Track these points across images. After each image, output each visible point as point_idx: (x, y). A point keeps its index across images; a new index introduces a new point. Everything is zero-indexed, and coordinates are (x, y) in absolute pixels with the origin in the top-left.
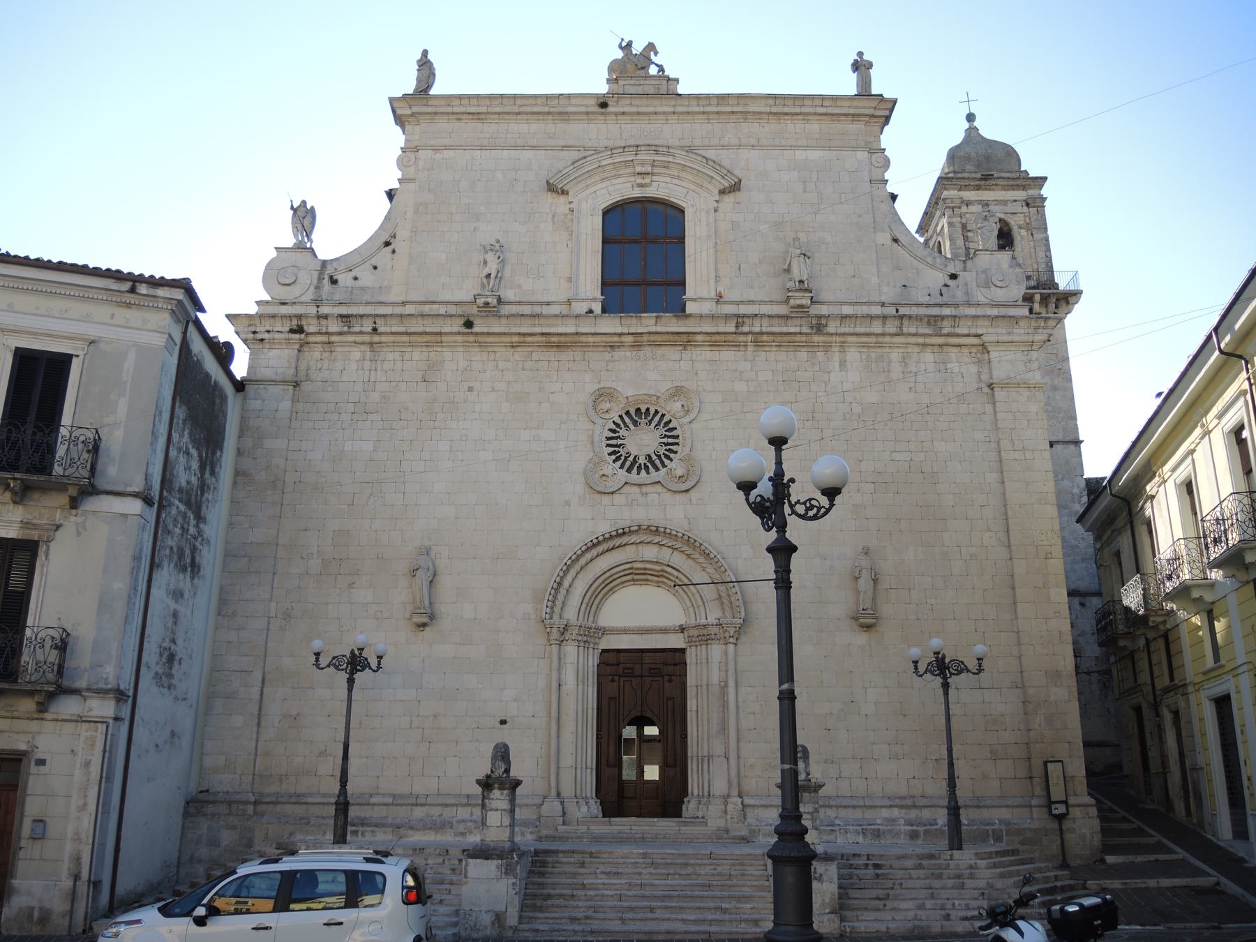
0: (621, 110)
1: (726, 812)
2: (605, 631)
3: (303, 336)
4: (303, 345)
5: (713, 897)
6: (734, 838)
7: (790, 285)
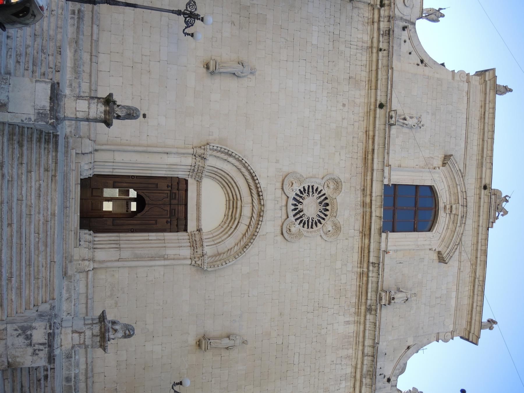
0: (482, 197)
1: (83, 260)
2: (199, 182)
3: (379, 6)
4: (373, 6)
5: (20, 270)
6: (66, 268)
7: (393, 292)
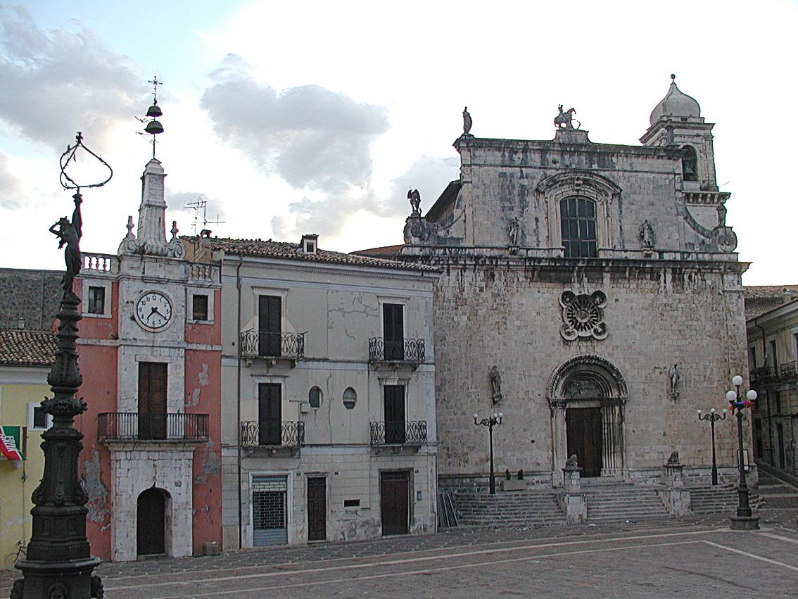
1: (622, 474)
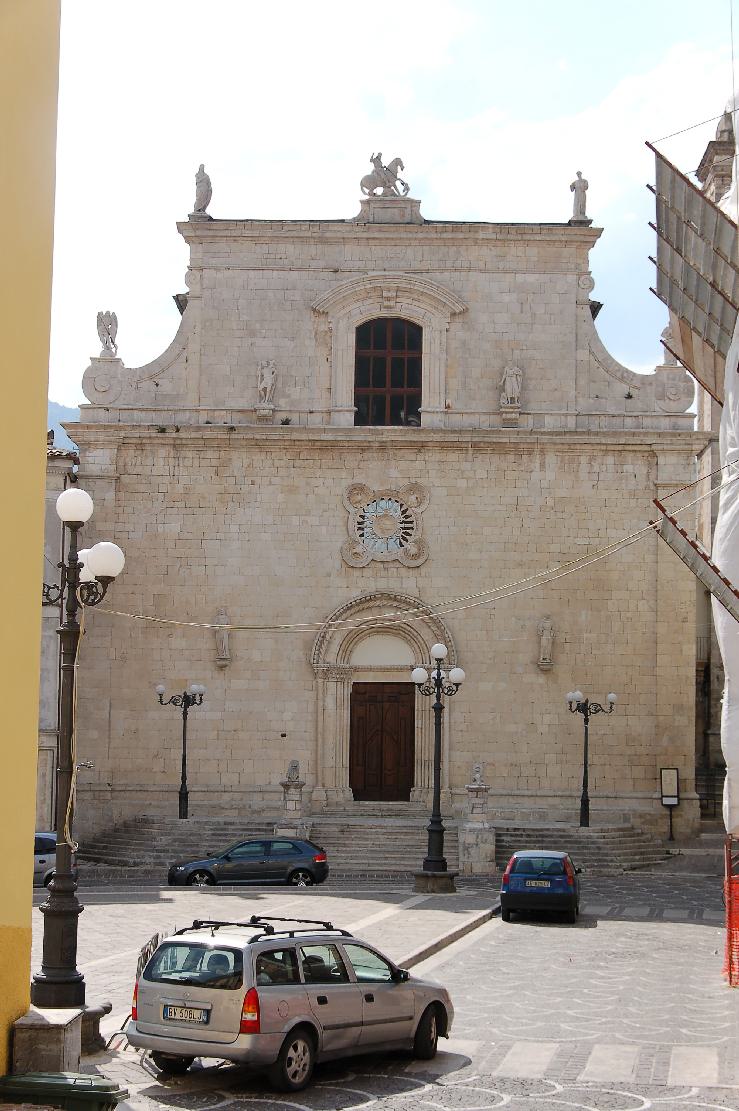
2: (356, 669)
